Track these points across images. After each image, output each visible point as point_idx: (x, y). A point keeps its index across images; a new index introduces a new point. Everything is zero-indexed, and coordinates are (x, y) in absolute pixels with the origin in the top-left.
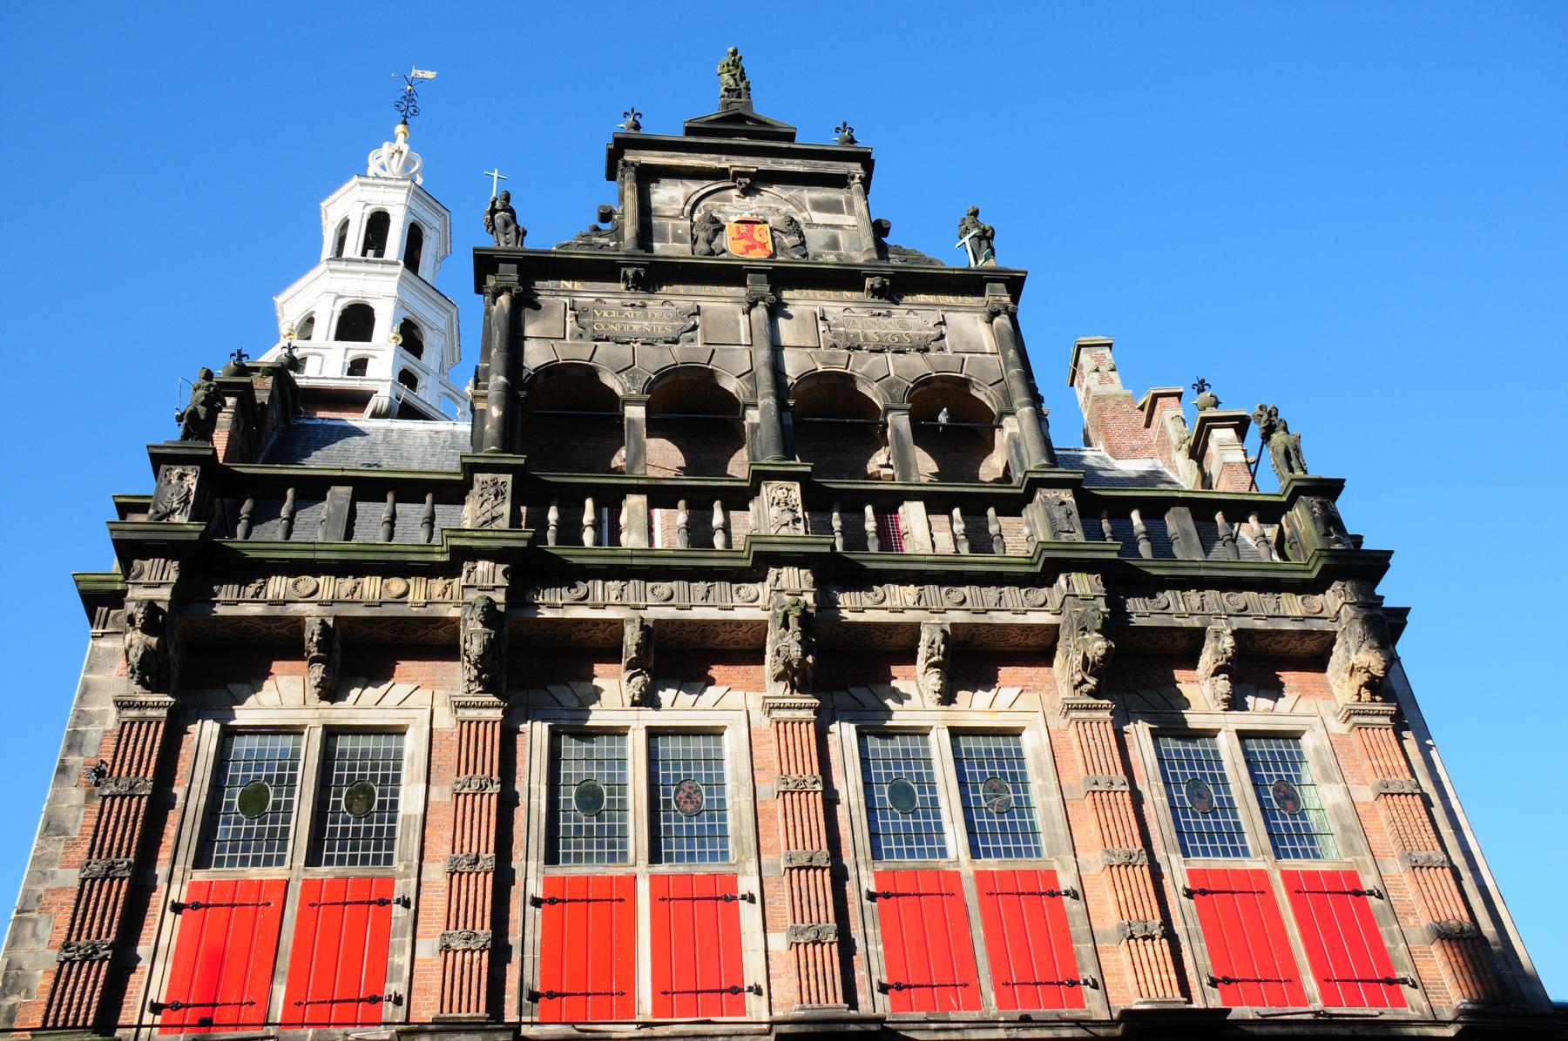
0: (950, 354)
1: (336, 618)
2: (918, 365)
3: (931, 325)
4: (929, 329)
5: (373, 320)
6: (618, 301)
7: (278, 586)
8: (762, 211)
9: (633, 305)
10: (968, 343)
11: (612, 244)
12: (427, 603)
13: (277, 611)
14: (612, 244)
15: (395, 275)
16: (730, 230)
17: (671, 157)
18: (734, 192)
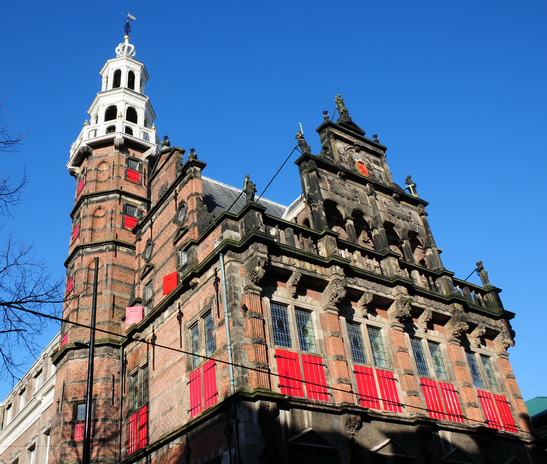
5: (137, 116)
6: (337, 181)
7: (285, 259)
9: (342, 184)
11: (331, 160)
12: (322, 275)
13: (286, 267)
15: (145, 101)
17: (340, 133)
18: (354, 150)
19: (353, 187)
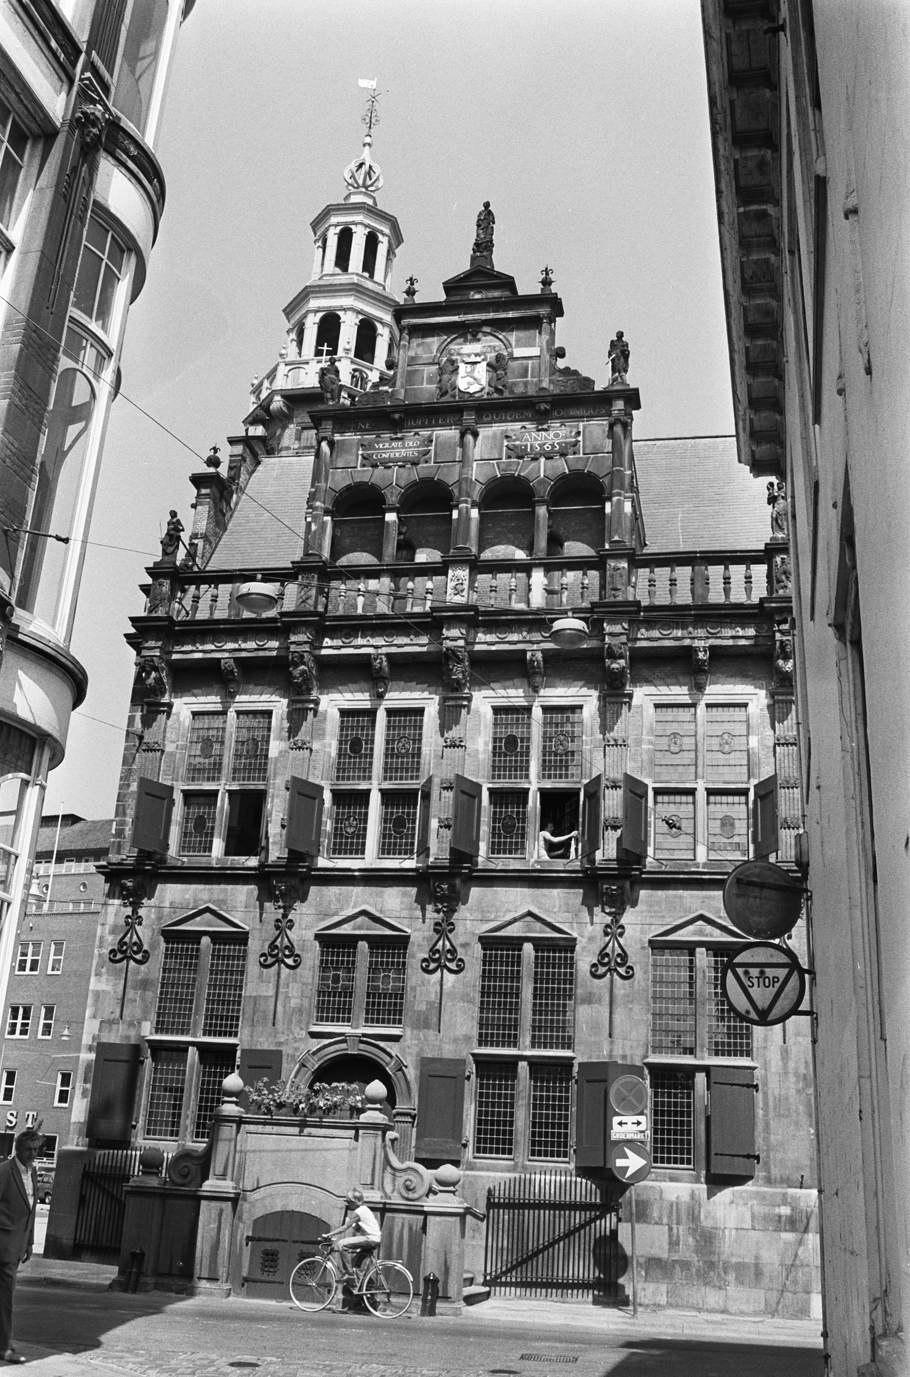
0: (581, 455)
1: (235, 659)
2: (561, 466)
3: (573, 434)
4: (571, 437)
8: (485, 350)
10: (594, 447)
14: (390, 390)
16: (463, 368)
19: (425, 433)
